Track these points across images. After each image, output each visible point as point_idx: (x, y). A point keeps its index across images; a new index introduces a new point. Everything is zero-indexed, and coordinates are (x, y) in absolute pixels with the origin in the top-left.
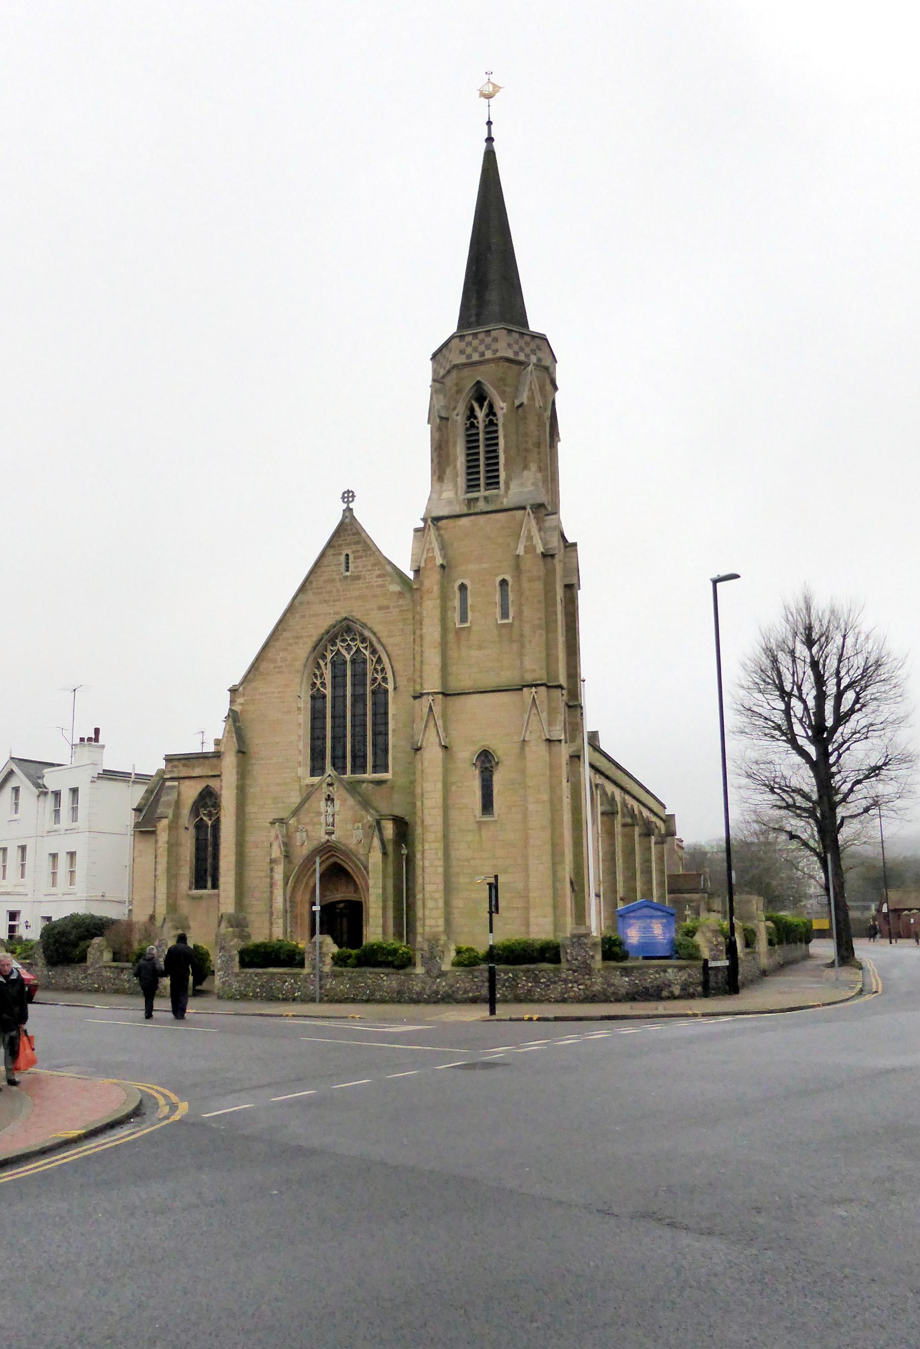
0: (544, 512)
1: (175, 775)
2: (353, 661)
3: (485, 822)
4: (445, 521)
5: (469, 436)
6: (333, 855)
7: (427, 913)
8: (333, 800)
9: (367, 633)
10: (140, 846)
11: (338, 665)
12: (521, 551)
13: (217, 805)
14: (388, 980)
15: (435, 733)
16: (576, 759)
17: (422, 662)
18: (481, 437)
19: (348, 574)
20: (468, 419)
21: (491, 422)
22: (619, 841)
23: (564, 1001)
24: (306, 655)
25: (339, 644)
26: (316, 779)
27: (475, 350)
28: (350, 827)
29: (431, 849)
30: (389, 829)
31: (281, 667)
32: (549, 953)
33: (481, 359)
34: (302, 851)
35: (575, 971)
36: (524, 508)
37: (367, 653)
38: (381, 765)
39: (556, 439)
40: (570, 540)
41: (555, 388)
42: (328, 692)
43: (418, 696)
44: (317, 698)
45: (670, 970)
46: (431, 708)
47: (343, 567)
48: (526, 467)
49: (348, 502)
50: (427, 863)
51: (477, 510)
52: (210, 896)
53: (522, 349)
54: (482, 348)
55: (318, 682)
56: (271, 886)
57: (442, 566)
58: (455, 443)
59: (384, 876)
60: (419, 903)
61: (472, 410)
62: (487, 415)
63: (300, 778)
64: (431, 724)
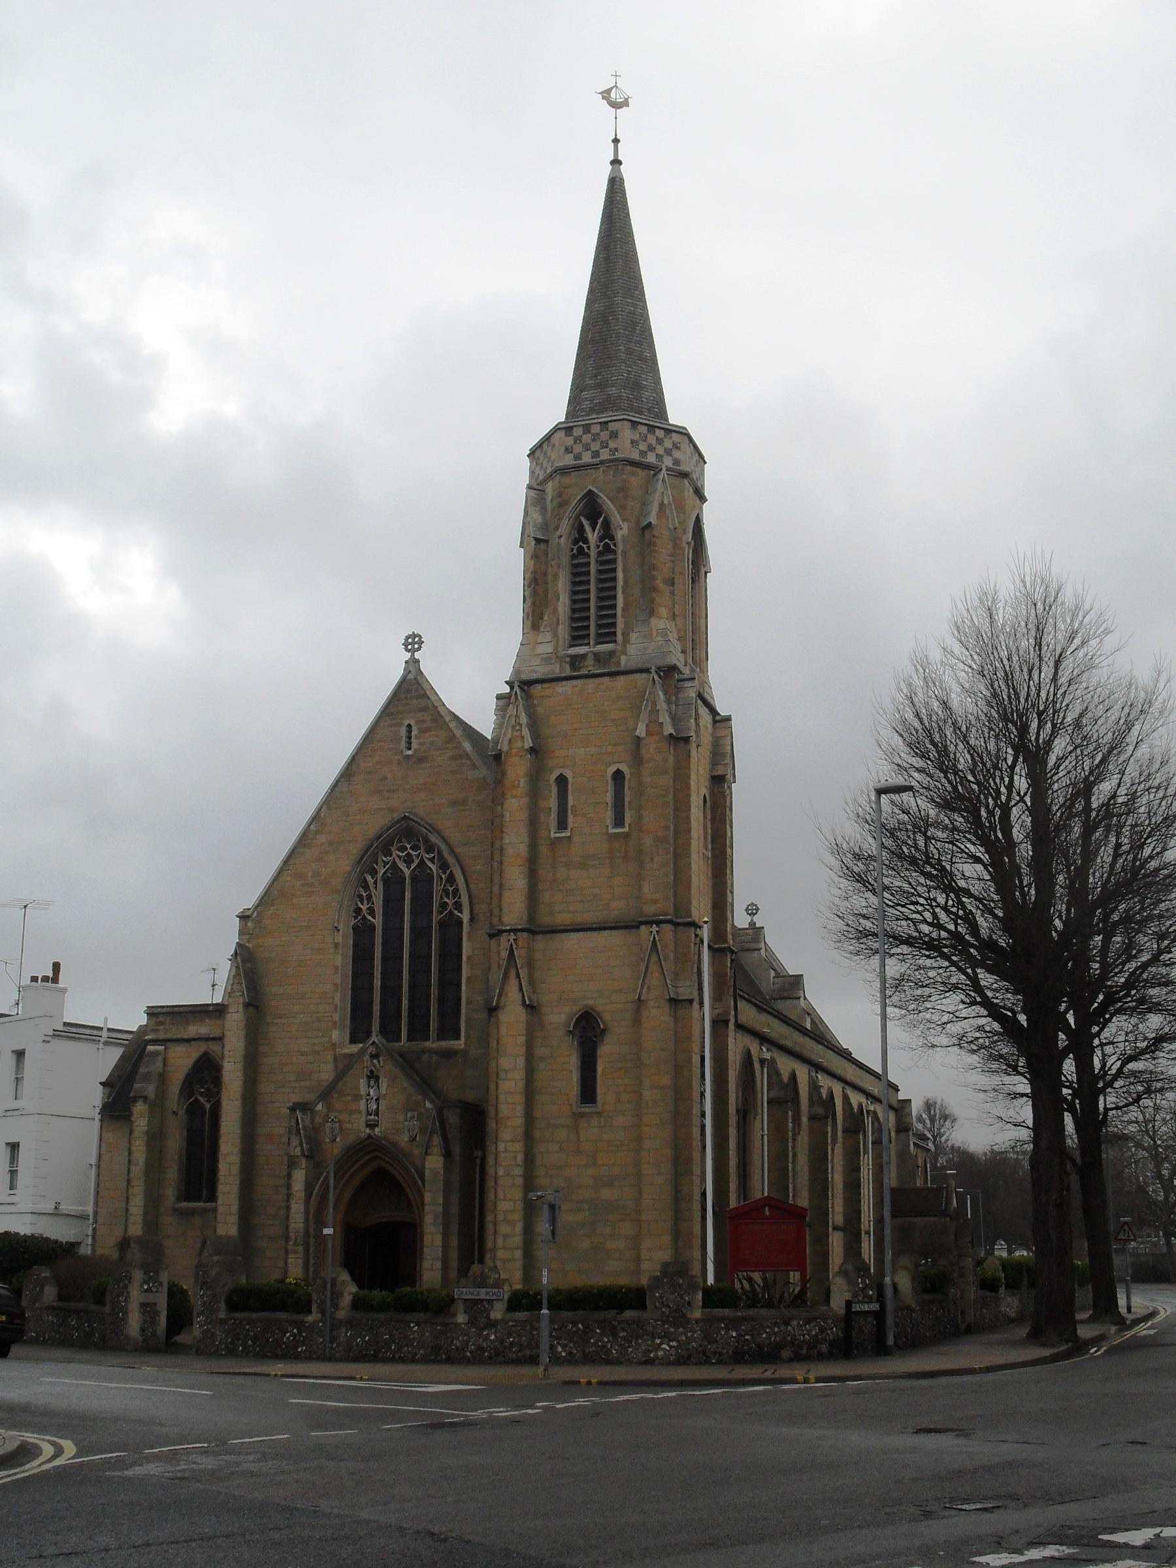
1: (161, 1036)
2: (414, 878)
3: (583, 1115)
4: (539, 687)
5: (575, 566)
6: (377, 1157)
7: (500, 1242)
8: (377, 1078)
9: (434, 839)
10: (110, 1137)
11: (393, 882)
12: (641, 731)
13: (217, 1081)
14: (416, 1329)
15: (517, 988)
17: (501, 885)
18: (593, 569)
19: (410, 753)
20: (576, 542)
21: (607, 546)
23: (649, 1362)
24: (349, 868)
25: (395, 853)
26: (355, 1048)
28: (400, 1117)
29: (506, 1151)
30: (453, 1119)
31: (312, 885)
32: (635, 1298)
33: (596, 460)
34: (334, 1149)
35: (664, 1323)
36: (647, 671)
37: (433, 867)
38: (450, 1029)
39: (703, 570)
40: (723, 711)
41: (703, 499)
42: (378, 921)
43: (495, 934)
44: (362, 932)
46: (512, 950)
47: (403, 745)
48: (652, 612)
49: (413, 651)
50: (501, 1172)
51: (584, 672)
52: (205, 1211)
53: (651, 448)
54: (595, 447)
55: (364, 907)
56: (288, 1200)
57: (532, 750)
58: (556, 576)
59: (447, 1191)
60: (490, 1228)
61: (581, 530)
62: (601, 539)
63: (334, 1045)
64: (513, 973)
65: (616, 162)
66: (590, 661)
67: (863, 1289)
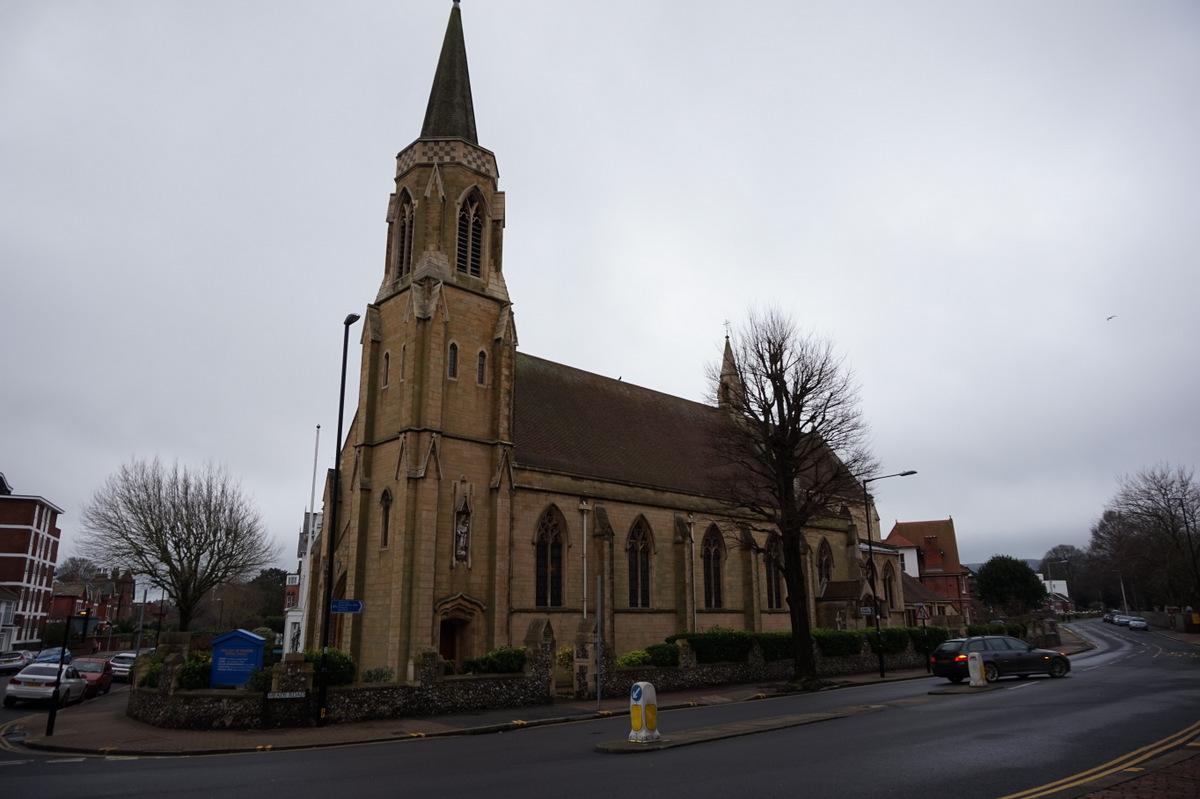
0: (433, 283)
39: (488, 220)
45: (225, 701)
53: (436, 154)
57: (373, 341)
61: (404, 211)
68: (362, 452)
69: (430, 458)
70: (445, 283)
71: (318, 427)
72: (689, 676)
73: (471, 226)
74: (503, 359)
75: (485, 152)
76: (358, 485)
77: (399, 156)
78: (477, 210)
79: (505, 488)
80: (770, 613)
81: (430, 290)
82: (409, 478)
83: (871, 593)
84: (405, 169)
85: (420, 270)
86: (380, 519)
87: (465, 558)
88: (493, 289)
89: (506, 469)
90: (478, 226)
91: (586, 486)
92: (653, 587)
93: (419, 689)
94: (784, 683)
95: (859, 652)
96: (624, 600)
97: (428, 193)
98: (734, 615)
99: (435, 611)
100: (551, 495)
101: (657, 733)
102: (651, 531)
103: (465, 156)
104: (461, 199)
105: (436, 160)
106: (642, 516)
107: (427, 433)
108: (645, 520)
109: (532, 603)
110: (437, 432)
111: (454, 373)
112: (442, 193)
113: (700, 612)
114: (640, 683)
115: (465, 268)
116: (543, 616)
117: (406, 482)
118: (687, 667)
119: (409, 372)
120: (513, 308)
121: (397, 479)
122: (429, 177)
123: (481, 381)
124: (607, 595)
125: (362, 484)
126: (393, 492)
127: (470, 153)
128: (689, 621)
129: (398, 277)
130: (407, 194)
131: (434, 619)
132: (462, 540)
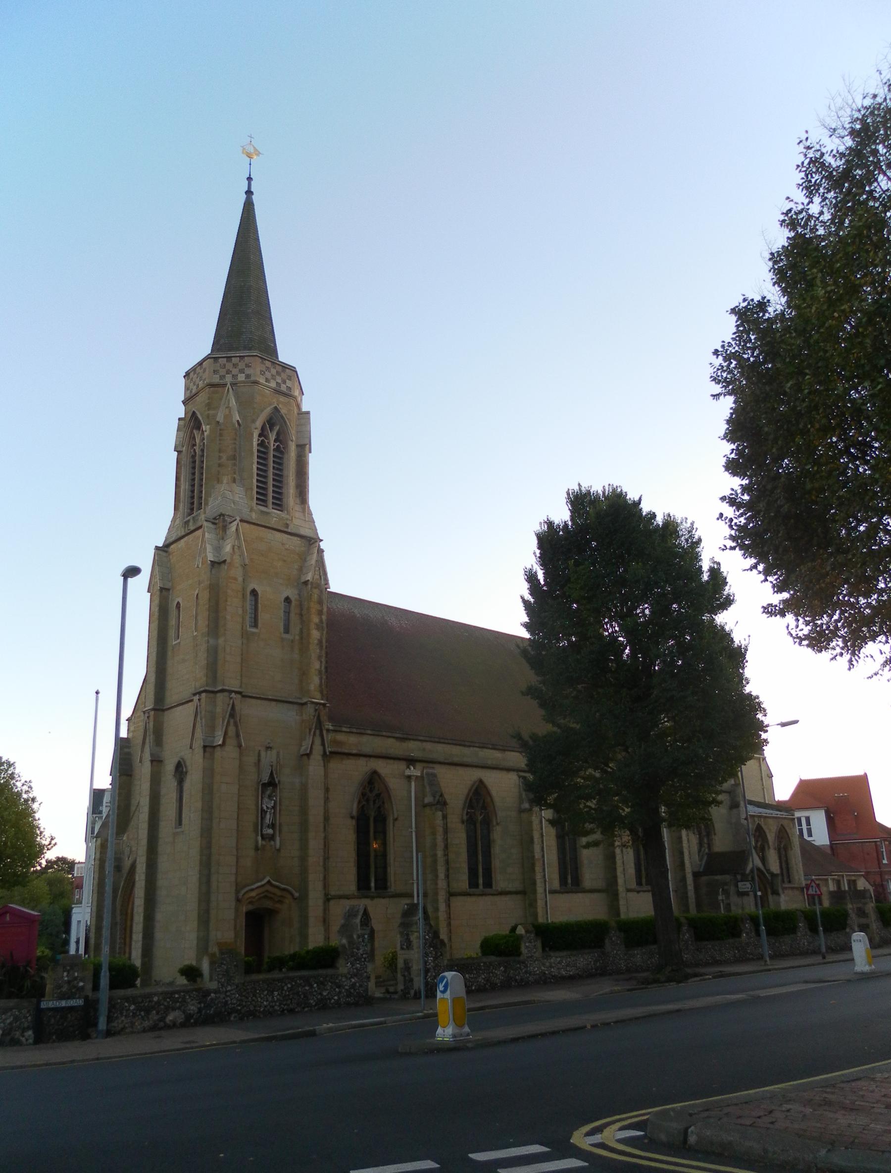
4: (172, 546)
16: (305, 757)
22: (315, 844)
27: (194, 384)
48: (219, 481)
61: (194, 438)
65: (249, 193)
66: (191, 524)
67: (69, 982)
68: (152, 718)
69: (228, 722)
70: (241, 521)
71: (97, 693)
72: (535, 968)
73: (272, 453)
74: (312, 604)
75: (285, 367)
76: (147, 756)
77: (187, 375)
78: (278, 434)
79: (318, 748)
80: (638, 892)
81: (225, 528)
82: (205, 747)
83: (760, 865)
84: (194, 391)
85: (213, 506)
86: (174, 795)
87: (272, 838)
88: (297, 524)
89: (318, 732)
90: (280, 451)
91: (413, 748)
92: (496, 863)
93: (215, 992)
94: (645, 974)
95: (739, 935)
96: (462, 881)
97: (220, 418)
98: (595, 896)
99: (238, 900)
100: (372, 759)
101: (467, 1029)
102: (492, 800)
103: (262, 373)
104: (259, 423)
105: (229, 379)
106: (481, 781)
107: (226, 694)
108: (485, 787)
109: (352, 888)
110: (236, 692)
111: (255, 625)
112: (236, 417)
113: (552, 892)
114: (446, 974)
115: (265, 501)
116: (362, 903)
117: (202, 751)
118: (531, 957)
119: (203, 623)
120: (322, 545)
121: (191, 748)
122: (221, 399)
123: (287, 630)
124: (442, 876)
125: (152, 755)
126: (188, 763)
127: (268, 369)
128: (540, 903)
129: (190, 515)
130: (197, 419)
131: (237, 910)
132: (268, 816)
